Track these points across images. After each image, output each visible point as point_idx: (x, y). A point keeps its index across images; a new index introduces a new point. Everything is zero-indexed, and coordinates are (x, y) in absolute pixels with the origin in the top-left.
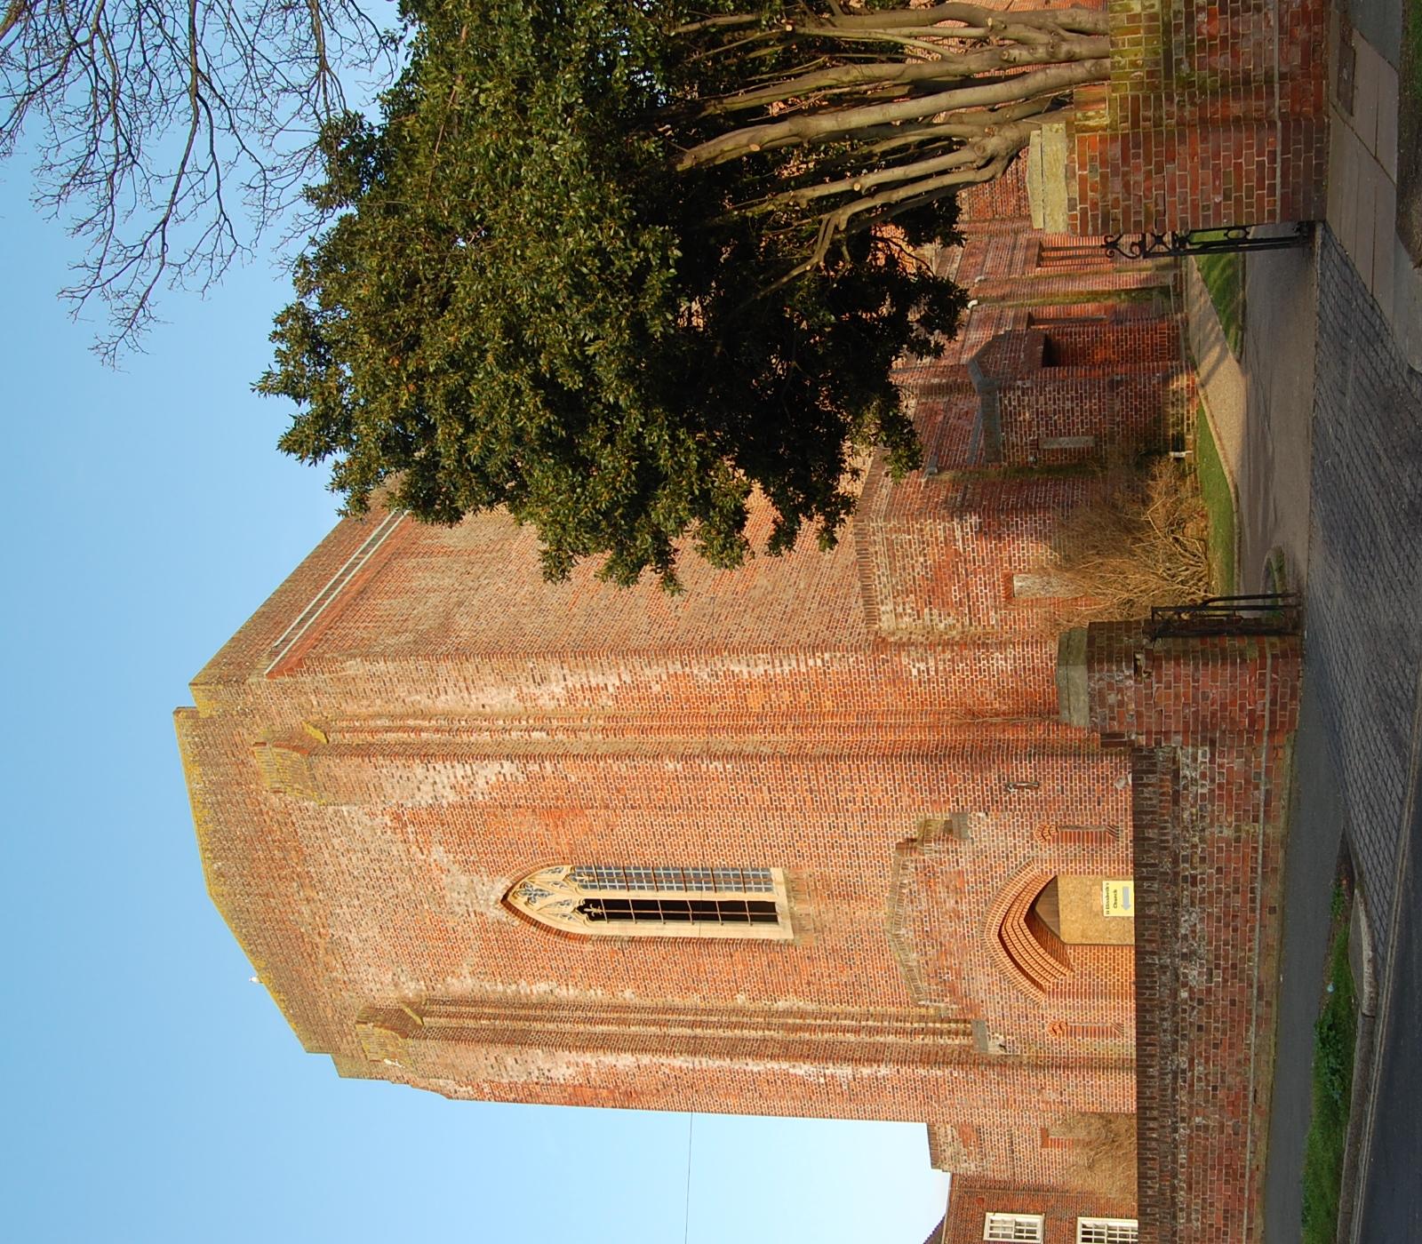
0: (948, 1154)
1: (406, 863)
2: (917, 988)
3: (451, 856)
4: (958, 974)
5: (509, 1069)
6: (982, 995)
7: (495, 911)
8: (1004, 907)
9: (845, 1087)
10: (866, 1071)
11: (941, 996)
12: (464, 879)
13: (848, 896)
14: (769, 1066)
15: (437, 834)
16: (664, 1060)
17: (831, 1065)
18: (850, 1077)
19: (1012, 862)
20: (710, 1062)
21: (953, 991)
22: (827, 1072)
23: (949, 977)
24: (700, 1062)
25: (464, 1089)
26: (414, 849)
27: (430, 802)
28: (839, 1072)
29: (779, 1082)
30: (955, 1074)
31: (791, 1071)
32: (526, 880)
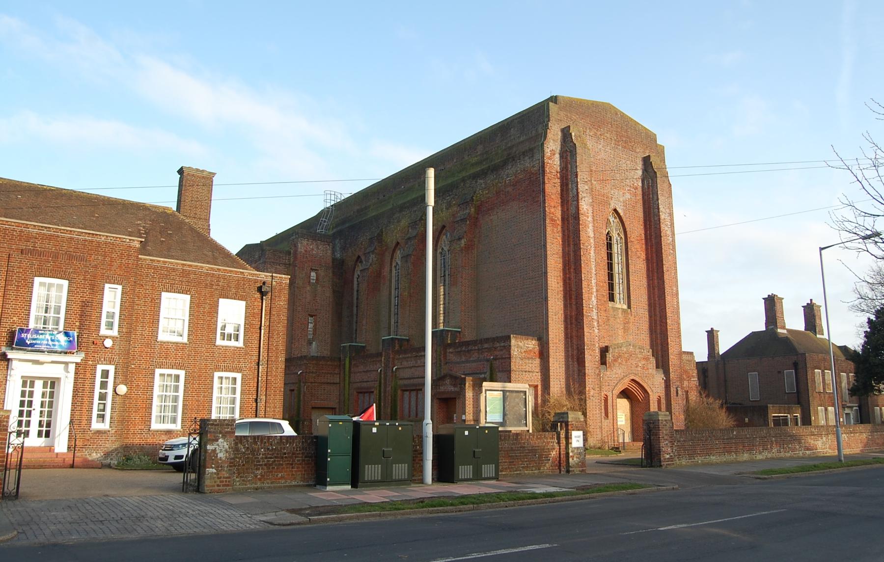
0: (520, 344)
1: (624, 182)
2: (615, 348)
3: (627, 199)
4: (620, 363)
5: (584, 185)
6: (615, 371)
7: (613, 206)
8: (641, 382)
9: (589, 314)
10: (595, 324)
11: (613, 356)
12: (621, 200)
13: (624, 328)
14: (594, 288)
15: (633, 198)
16: (593, 249)
17: (597, 311)
18: (593, 317)
19: (652, 386)
20: (594, 266)
21: (615, 361)
22: (594, 309)
23: (620, 361)
24: (593, 262)
25: (549, 152)
26: (629, 188)
27: (661, 209)
28: (595, 314)
29: (588, 289)
30: (597, 357)
31: (593, 296)
32: (618, 220)
